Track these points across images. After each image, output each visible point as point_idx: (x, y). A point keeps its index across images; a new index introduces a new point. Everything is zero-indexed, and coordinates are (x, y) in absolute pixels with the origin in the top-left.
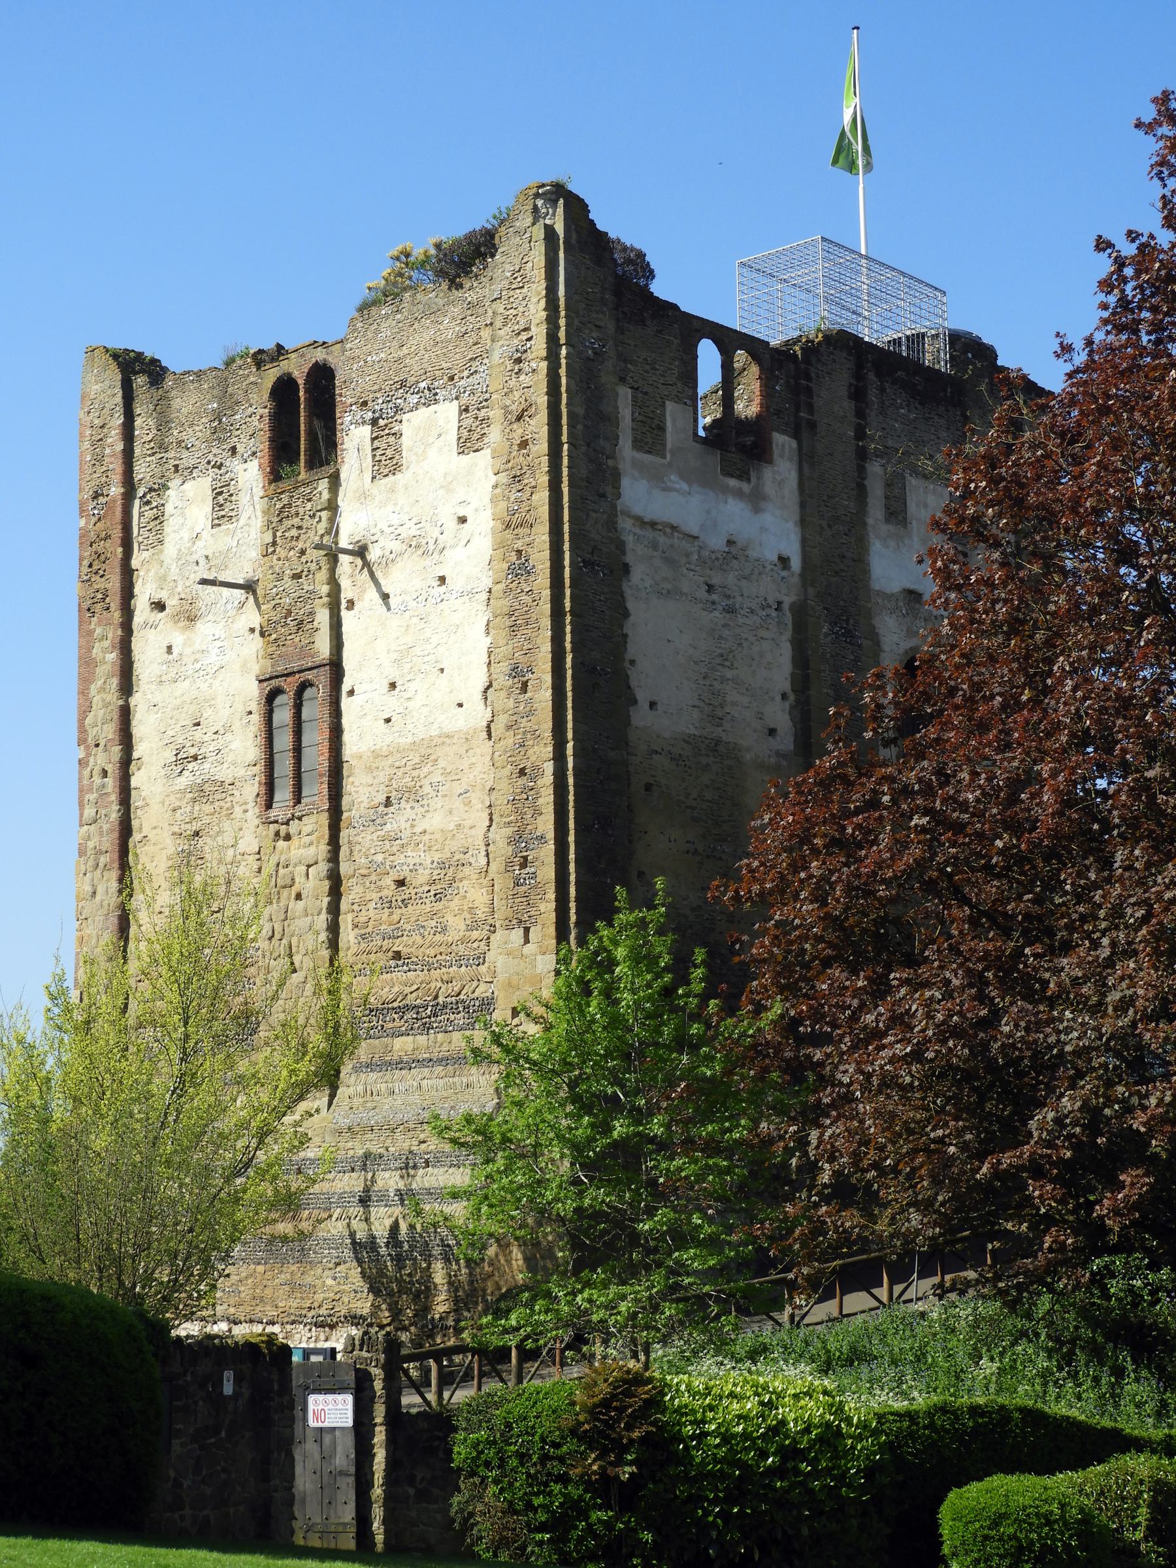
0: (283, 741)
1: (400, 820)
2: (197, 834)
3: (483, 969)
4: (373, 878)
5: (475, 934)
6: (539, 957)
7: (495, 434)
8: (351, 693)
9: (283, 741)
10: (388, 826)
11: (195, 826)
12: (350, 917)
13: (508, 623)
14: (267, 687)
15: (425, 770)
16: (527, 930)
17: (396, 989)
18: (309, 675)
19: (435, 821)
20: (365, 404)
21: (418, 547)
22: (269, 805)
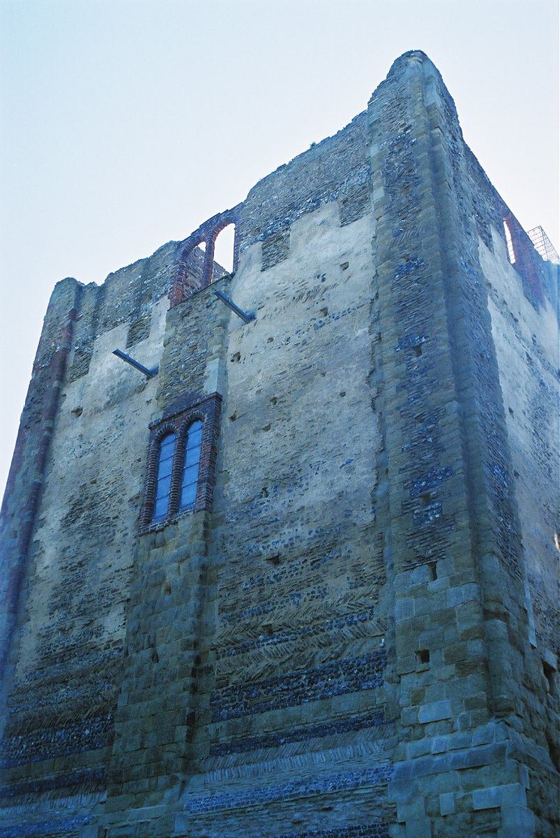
0: (166, 467)
1: (277, 505)
2: (80, 564)
3: (369, 624)
4: (245, 563)
5: (361, 590)
6: (451, 590)
7: (378, 194)
8: (233, 418)
9: (166, 467)
10: (263, 514)
11: (80, 558)
12: (217, 603)
13: (398, 309)
14: (157, 432)
15: (304, 458)
16: (433, 566)
17: (263, 664)
18: (196, 411)
19: (315, 494)
20: (259, 230)
21: (300, 297)
22: (148, 522)
